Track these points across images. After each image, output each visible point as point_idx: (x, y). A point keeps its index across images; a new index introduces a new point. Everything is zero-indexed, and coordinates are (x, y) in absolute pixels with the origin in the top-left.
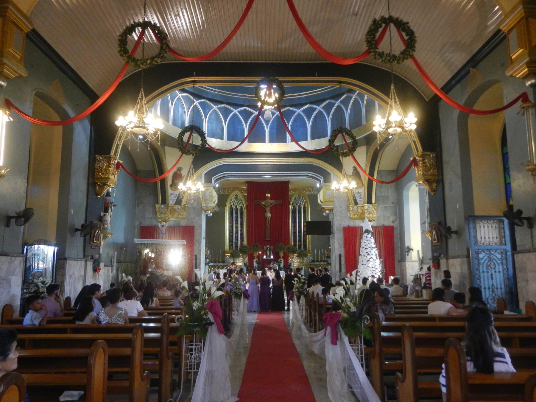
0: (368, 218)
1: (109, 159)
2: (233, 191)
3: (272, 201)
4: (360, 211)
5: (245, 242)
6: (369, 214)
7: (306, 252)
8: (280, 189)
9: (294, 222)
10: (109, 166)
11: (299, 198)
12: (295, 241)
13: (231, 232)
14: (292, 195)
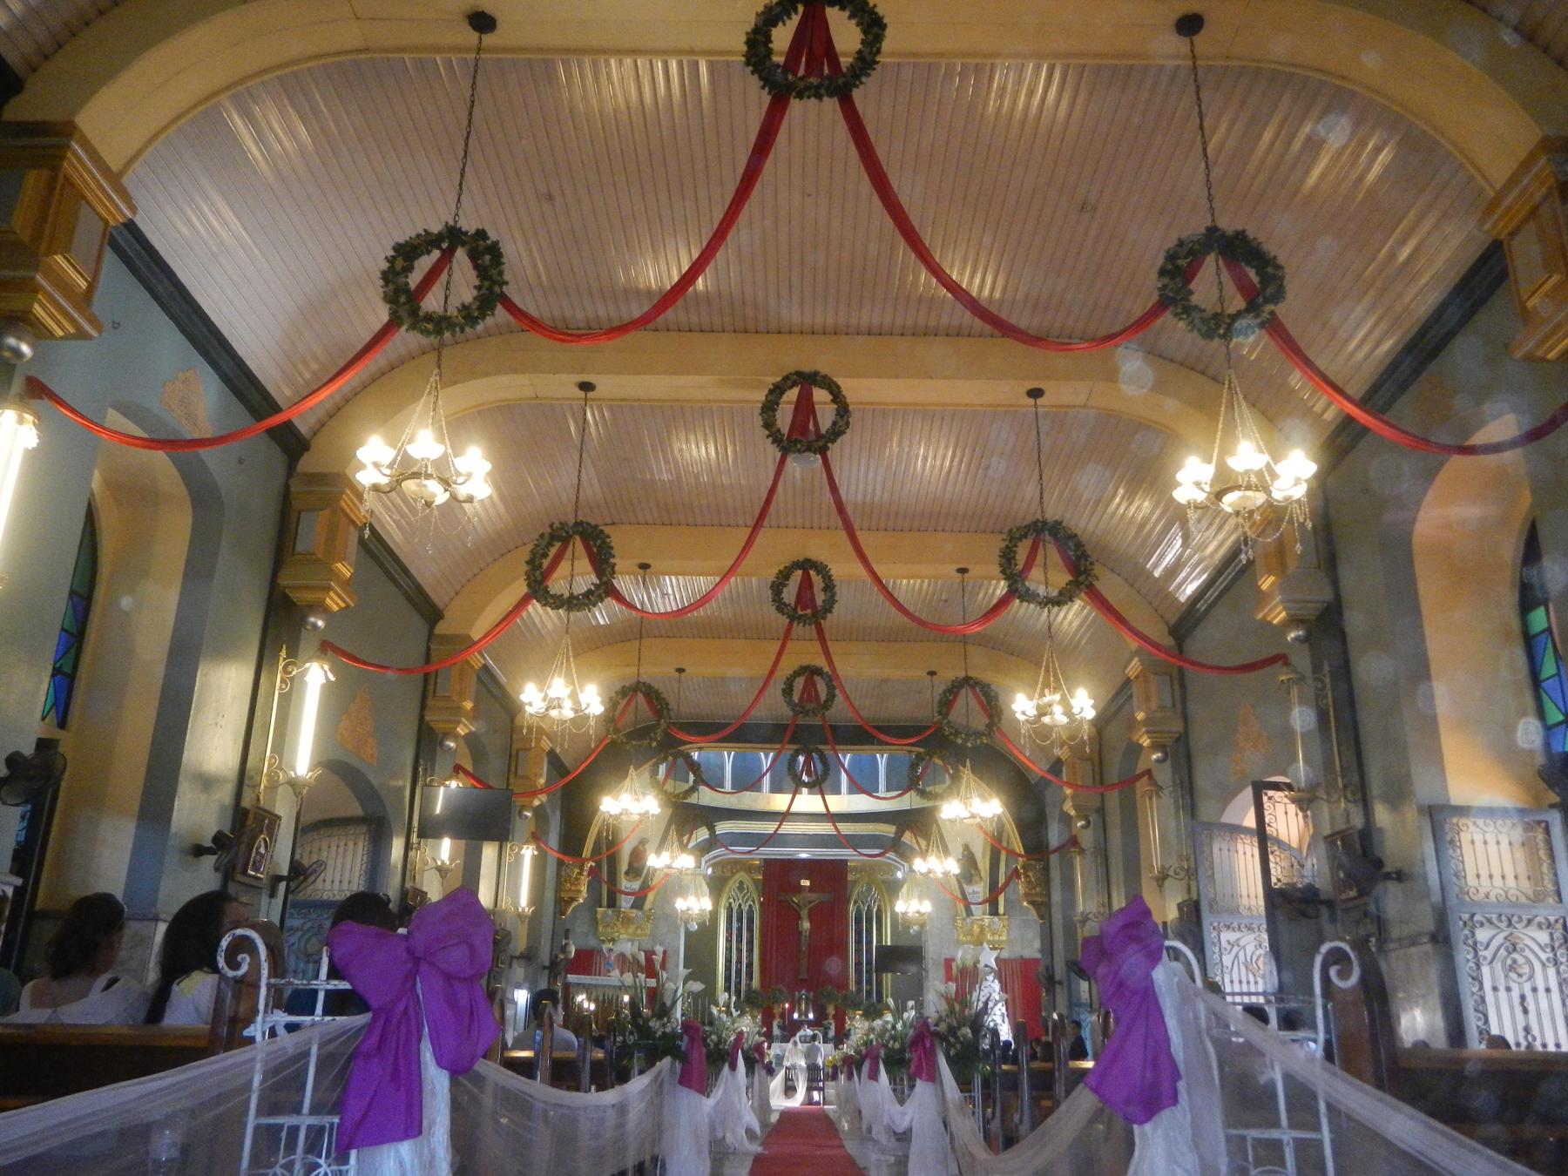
0: (989, 942)
2: (733, 874)
3: (813, 896)
4: (976, 929)
5: (756, 983)
8: (831, 876)
9: (859, 942)
10: (580, 874)
11: (869, 890)
12: (859, 982)
13: (728, 961)
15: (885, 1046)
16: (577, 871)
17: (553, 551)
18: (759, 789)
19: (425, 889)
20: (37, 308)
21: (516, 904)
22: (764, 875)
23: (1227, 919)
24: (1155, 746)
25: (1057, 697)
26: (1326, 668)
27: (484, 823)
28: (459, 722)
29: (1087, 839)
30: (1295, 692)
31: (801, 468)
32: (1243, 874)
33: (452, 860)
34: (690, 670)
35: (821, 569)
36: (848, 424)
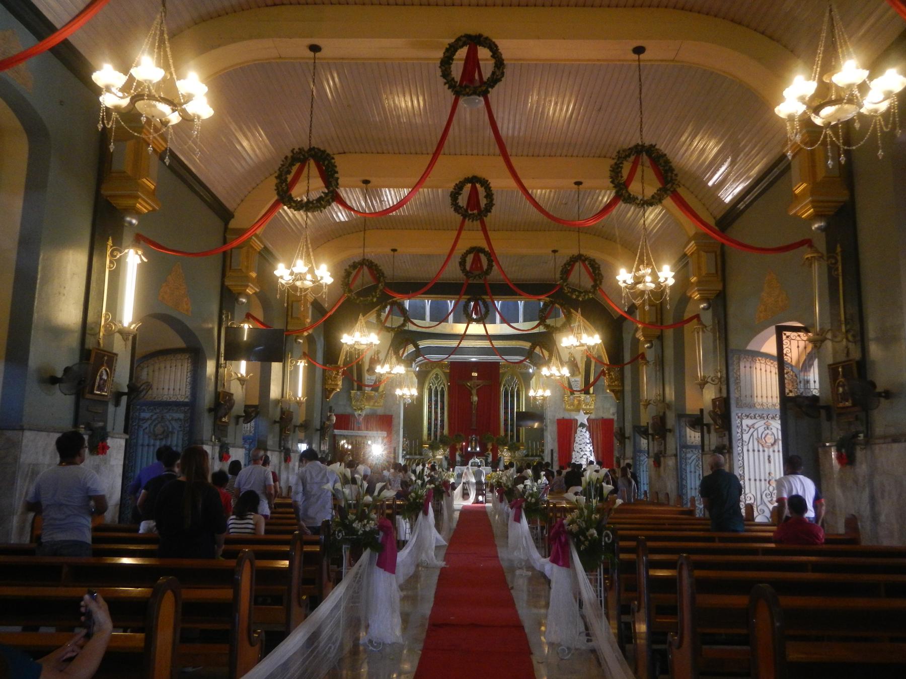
0: (584, 410)
3: (480, 381)
4: (576, 402)
5: (446, 431)
6: (586, 405)
7: (518, 444)
9: (506, 408)
10: (337, 374)
11: (512, 378)
12: (506, 430)
13: (430, 418)
14: (504, 374)
15: (526, 500)
16: (335, 373)
17: (294, 169)
18: (445, 320)
19: (232, 391)
21: (295, 395)
22: (451, 369)
23: (746, 411)
24: (702, 299)
25: (649, 271)
26: (839, 249)
27: (271, 348)
28: (247, 286)
29: (650, 355)
30: (816, 265)
31: (471, 109)
32: (763, 382)
33: (248, 373)
34: (399, 250)
35: (485, 183)
36: (503, 74)
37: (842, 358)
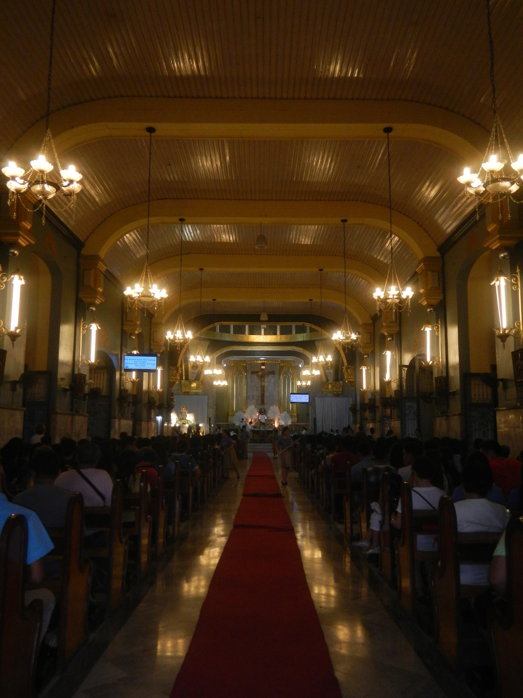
1: (177, 369)
10: (177, 372)
11: (289, 370)
18: (243, 333)
19: (127, 388)
20: (20, 241)
28: (136, 330)
34: (218, 300)
37: (440, 375)
